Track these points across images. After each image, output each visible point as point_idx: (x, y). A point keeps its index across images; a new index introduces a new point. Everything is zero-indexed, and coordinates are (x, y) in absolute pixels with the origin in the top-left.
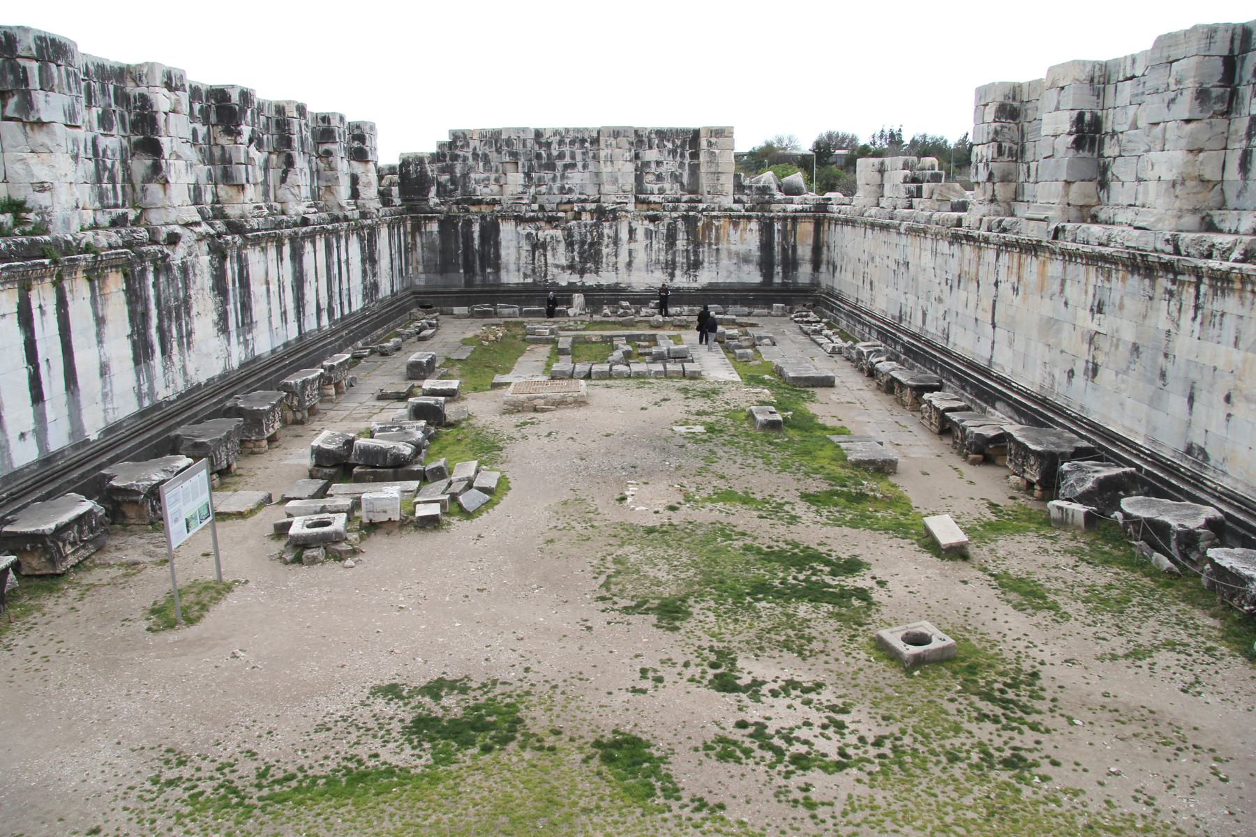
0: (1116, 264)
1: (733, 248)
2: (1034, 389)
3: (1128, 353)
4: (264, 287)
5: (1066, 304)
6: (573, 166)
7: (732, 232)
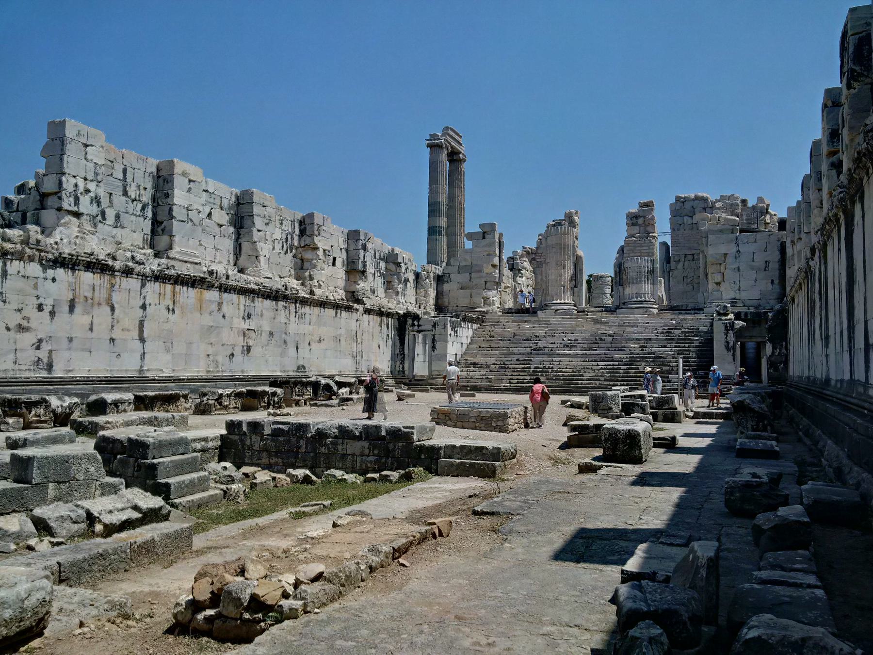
2: (203, 374)
5: (224, 316)
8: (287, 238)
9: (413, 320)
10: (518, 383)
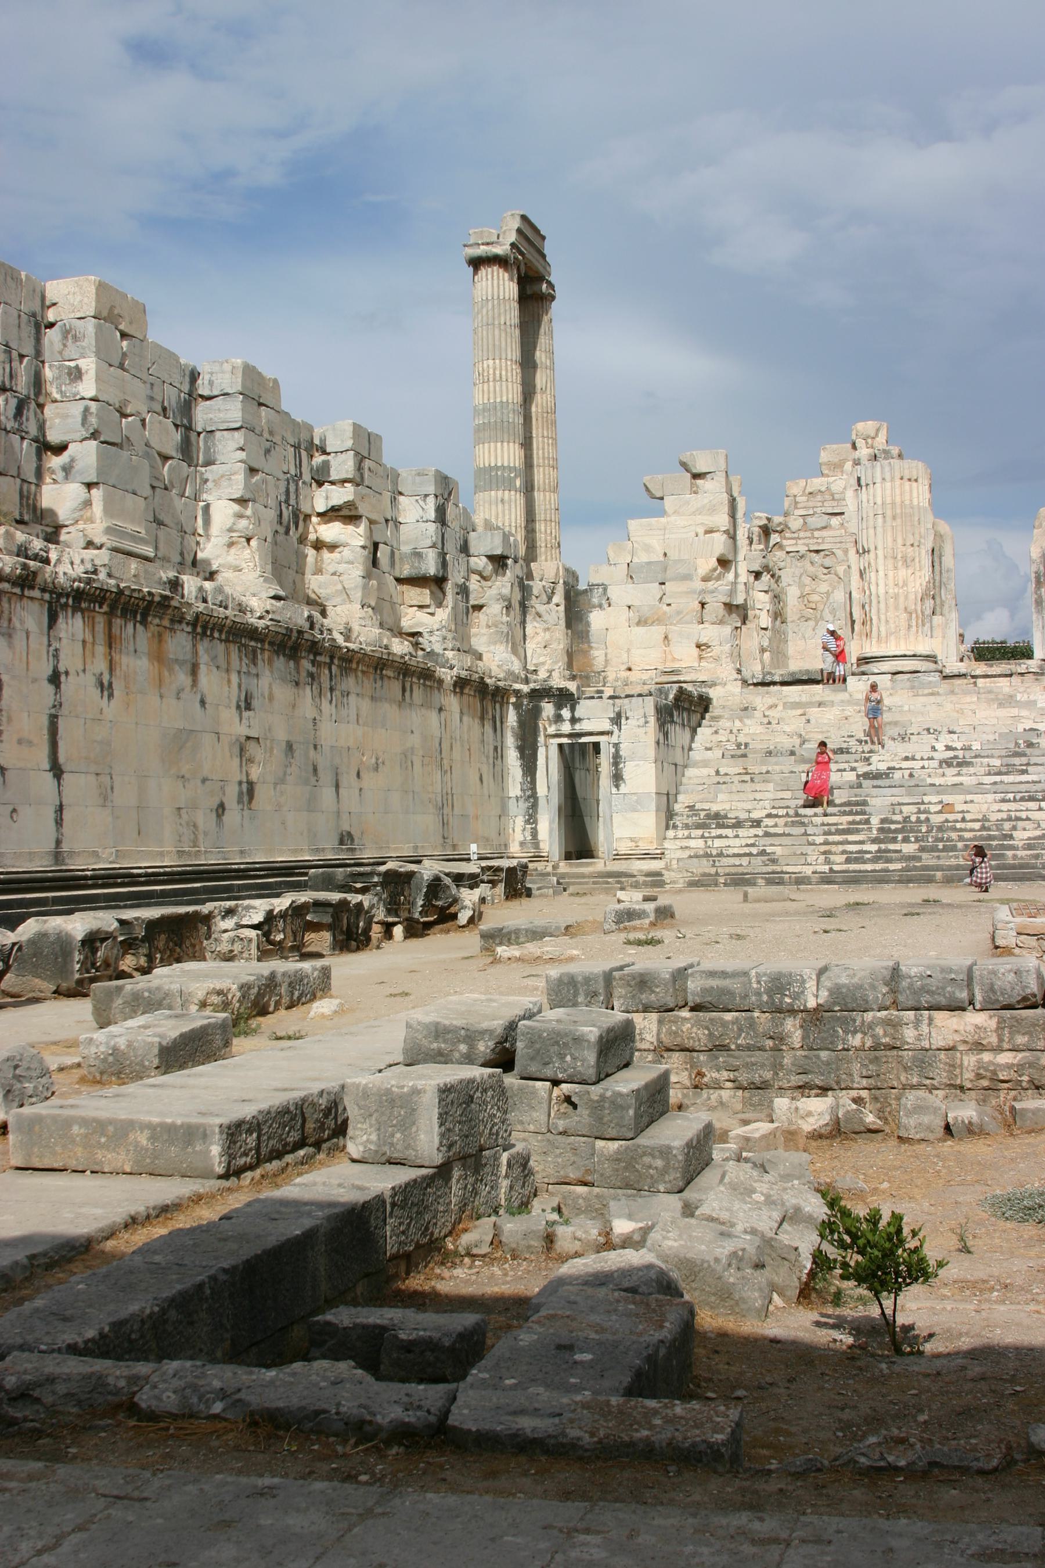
0: (262, 641)
2: (169, 862)
5: (203, 702)
8: (287, 492)
9: (559, 707)
10: (848, 861)
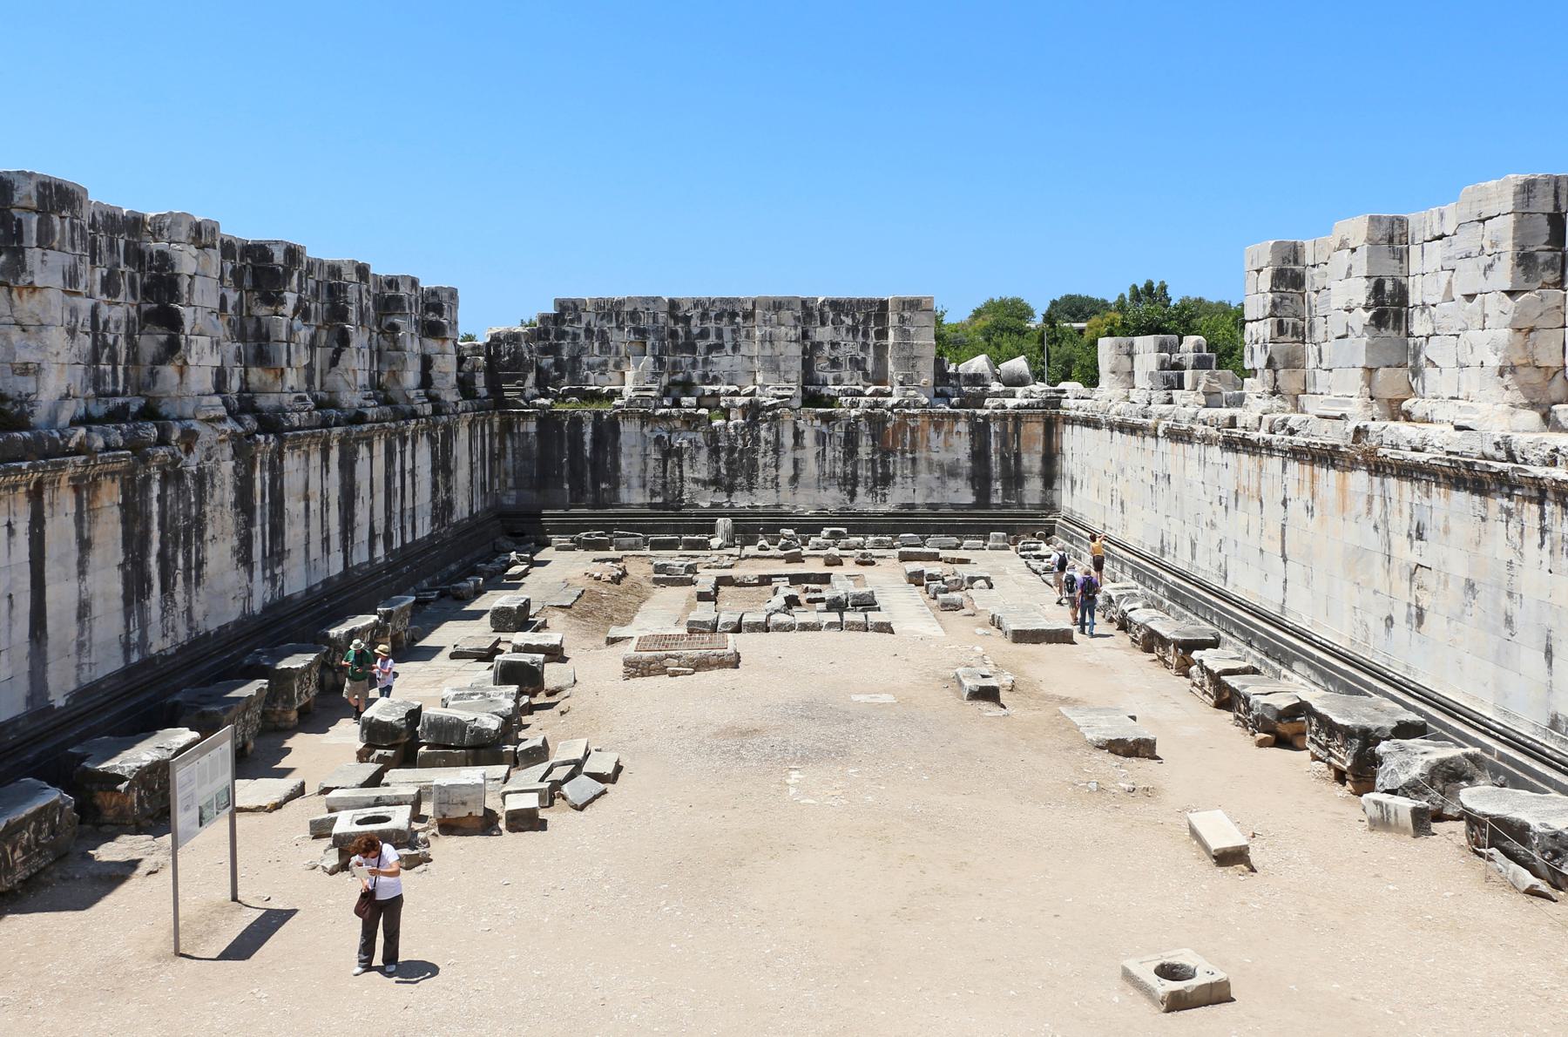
1: (935, 457)
2: (1343, 644)
3: (1460, 593)
4: (302, 504)
6: (719, 347)
7: (933, 435)
